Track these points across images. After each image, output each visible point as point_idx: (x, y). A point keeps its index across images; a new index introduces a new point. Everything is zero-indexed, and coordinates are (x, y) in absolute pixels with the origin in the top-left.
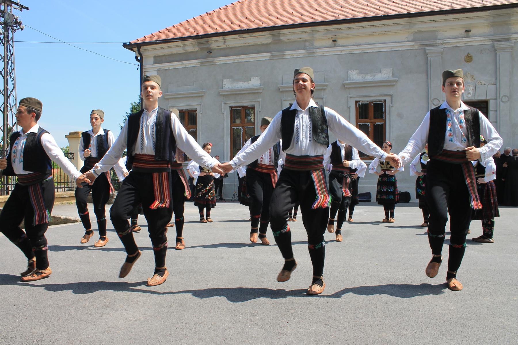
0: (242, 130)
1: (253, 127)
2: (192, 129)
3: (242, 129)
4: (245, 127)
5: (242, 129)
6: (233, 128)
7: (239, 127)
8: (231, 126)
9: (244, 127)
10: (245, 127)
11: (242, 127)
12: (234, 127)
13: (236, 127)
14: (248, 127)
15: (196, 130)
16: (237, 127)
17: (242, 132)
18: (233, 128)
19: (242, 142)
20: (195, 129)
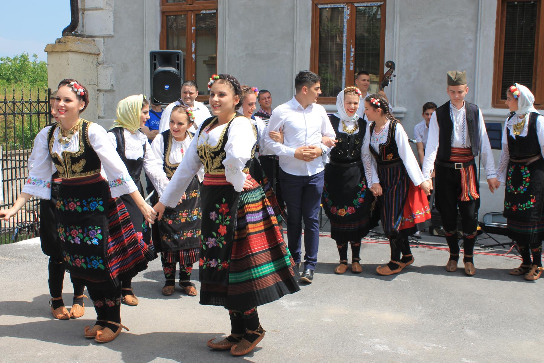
0: (345, 15)
1: (379, 3)
2: (204, 12)
3: (347, 11)
4: (356, 5)
5: (347, 11)
6: (320, 6)
7: (337, 6)
8: (316, 2)
9: (352, 3)
10: (356, 5)
11: (347, 3)
12: (321, 4)
13: (329, 6)
14: (365, 4)
15: (216, 14)
16: (332, 6)
17: (345, 21)
18: (320, 9)
19: (345, 48)
20: (215, 11)
